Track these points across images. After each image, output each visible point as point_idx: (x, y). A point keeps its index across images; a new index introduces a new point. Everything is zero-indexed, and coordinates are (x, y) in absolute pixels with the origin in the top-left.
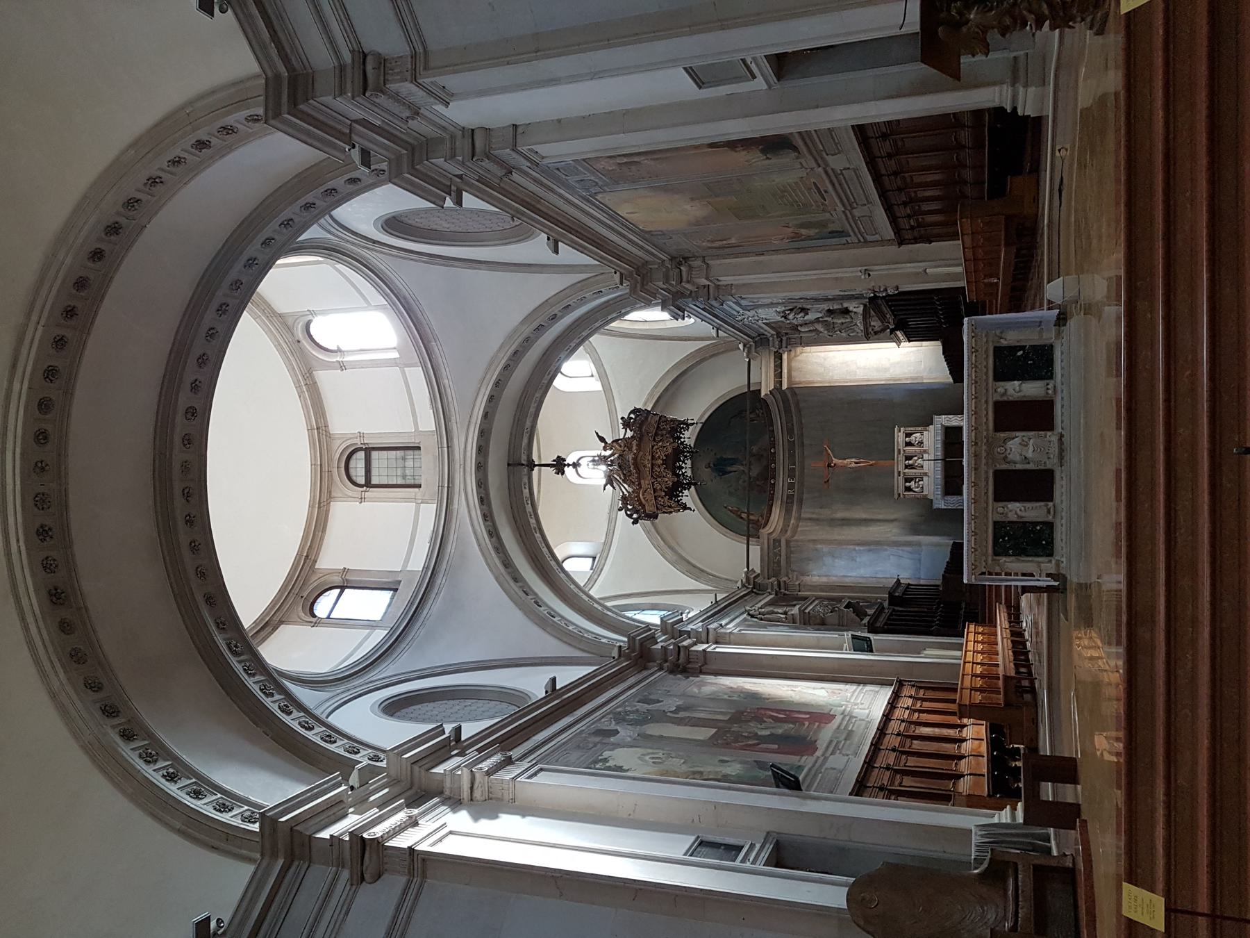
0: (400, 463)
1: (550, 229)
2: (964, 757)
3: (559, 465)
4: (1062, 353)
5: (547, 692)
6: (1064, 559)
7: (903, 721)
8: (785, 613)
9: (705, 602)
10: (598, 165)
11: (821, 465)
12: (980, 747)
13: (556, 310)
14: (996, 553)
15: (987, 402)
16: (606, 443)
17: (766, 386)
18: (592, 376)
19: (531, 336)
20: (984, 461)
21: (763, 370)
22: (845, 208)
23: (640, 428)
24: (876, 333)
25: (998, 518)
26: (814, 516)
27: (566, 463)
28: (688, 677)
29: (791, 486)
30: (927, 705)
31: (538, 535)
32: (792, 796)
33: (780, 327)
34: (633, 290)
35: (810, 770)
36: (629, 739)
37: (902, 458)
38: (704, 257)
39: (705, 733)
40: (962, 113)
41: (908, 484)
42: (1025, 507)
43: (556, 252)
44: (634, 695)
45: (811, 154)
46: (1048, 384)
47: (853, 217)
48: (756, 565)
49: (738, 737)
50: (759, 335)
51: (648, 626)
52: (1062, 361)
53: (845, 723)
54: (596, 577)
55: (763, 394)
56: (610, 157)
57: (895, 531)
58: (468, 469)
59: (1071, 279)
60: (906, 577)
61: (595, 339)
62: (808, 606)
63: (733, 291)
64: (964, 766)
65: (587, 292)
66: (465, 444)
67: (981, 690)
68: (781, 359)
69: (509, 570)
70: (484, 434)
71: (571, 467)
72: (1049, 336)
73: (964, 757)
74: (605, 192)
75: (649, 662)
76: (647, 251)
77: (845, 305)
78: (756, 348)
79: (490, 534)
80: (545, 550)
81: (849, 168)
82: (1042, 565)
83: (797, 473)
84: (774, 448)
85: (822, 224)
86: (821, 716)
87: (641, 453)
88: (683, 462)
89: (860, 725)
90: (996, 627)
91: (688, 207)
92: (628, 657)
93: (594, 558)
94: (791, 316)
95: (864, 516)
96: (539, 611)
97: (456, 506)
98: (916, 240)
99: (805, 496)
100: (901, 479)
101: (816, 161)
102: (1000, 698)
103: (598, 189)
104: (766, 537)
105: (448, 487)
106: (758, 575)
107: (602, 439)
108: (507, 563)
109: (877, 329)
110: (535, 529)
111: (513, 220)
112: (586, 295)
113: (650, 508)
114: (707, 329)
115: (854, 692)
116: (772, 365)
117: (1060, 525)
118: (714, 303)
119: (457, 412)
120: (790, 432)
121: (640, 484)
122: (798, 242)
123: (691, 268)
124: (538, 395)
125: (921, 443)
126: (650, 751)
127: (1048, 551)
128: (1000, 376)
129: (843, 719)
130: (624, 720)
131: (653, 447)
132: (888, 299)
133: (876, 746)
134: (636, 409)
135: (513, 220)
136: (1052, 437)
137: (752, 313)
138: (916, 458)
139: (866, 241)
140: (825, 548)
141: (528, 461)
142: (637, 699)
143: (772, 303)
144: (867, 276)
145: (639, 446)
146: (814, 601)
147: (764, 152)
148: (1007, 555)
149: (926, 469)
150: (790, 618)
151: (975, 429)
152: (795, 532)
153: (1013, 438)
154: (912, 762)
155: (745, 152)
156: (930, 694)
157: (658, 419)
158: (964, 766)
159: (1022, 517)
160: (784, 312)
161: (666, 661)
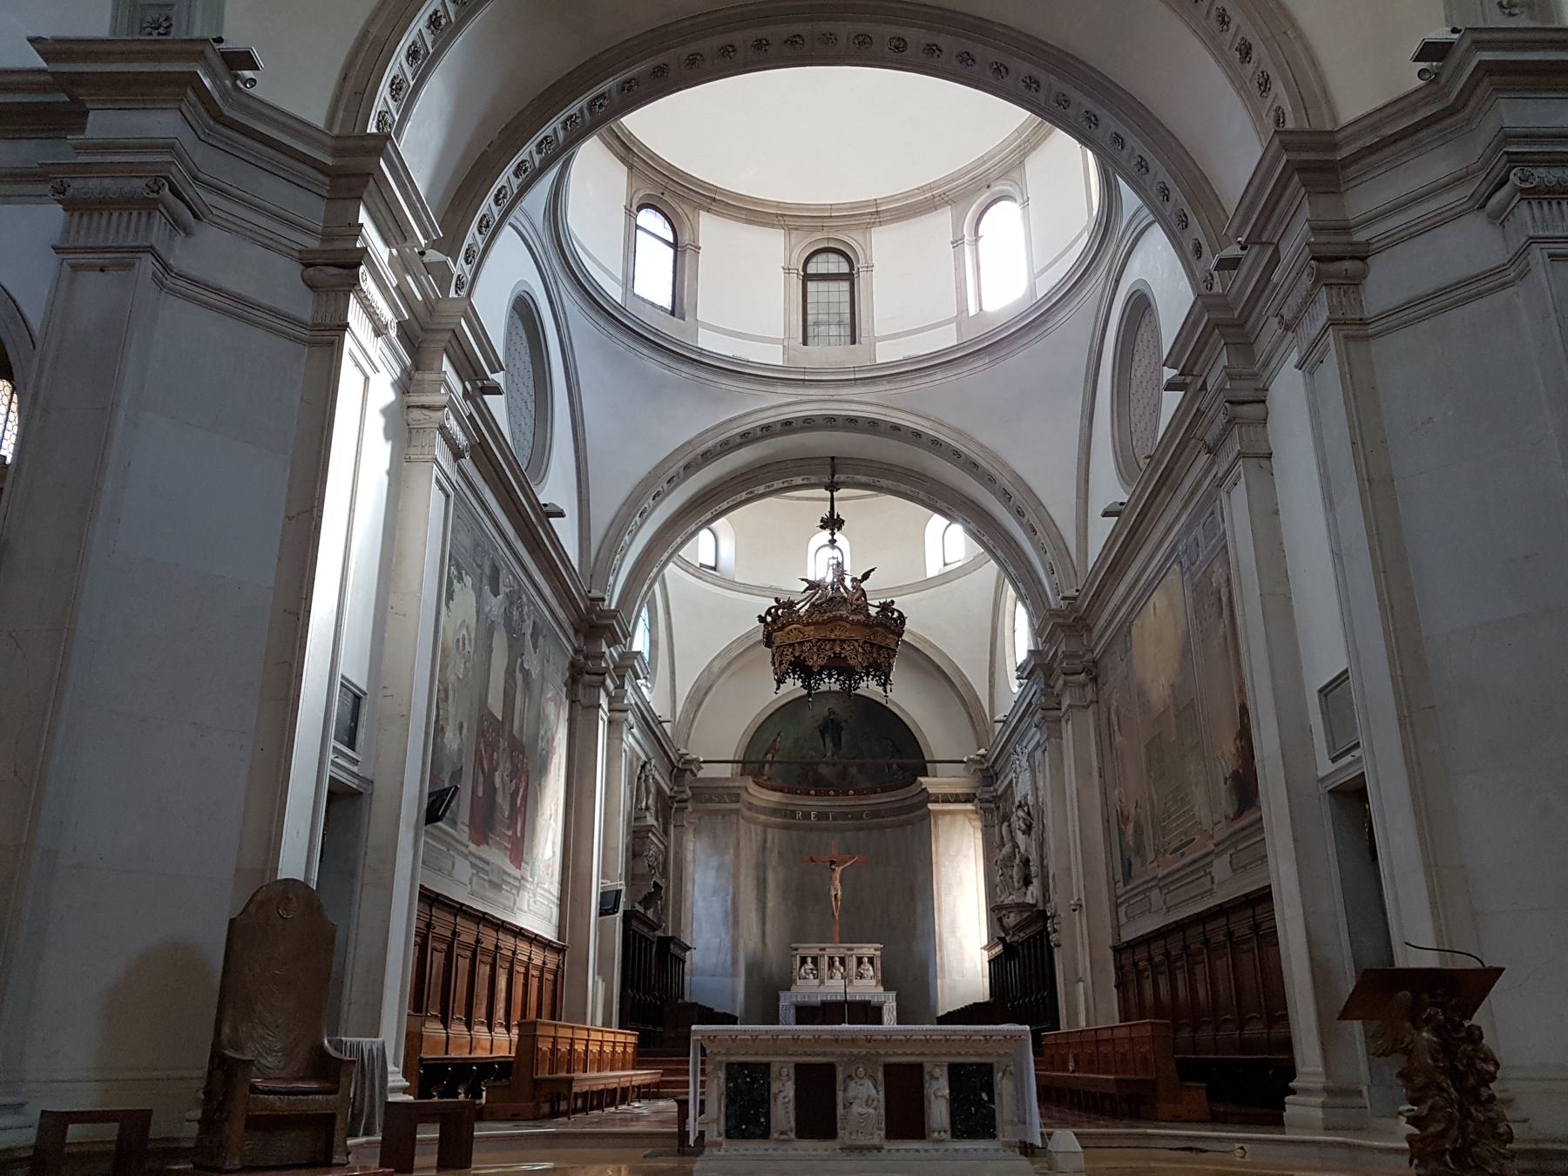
0: (835, 318)
1: (1135, 506)
2: (469, 1028)
3: (833, 523)
4: (985, 1150)
5: (545, 505)
6: (722, 1152)
7: (514, 953)
8: (647, 808)
9: (660, 707)
10: (1218, 564)
11: (834, 852)
12: (483, 1049)
13: (1030, 516)
14: (729, 1066)
15: (922, 1054)
16: (861, 581)
17: (932, 784)
18: (945, 565)
19: (997, 485)
20: (847, 1051)
21: (953, 779)
22: (1160, 880)
23: (880, 624)
24: (1000, 920)
25: (774, 1070)
26: (769, 844)
27: (836, 530)
28: (566, 685)
30: (534, 983)
31: (744, 496)
32: (419, 812)
33: (1006, 801)
34: (1054, 614)
35: (452, 836)
36: (487, 609)
37: (843, 952)
38: (1097, 702)
39: (496, 705)
40: (1288, 1026)
41: (809, 960)
42: (788, 1102)
43: (1106, 514)
44: (542, 616)
45: (1232, 835)
46: (945, 1132)
47: (1150, 889)
48: (707, 772)
49: (492, 747)
50: (996, 774)
51: (629, 635)
52: (976, 1150)
53: (511, 881)
54: (691, 570)
55: (922, 779)
56: (1228, 580)
57: (751, 945)
58: (828, 406)
59: (1080, 1162)
60: (694, 959)
61: (992, 567)
62: (657, 837)
63: (1053, 740)
64: (458, 1029)
65: (1052, 555)
66: (861, 402)
67: (554, 1050)
68: (967, 801)
69: (700, 460)
70: (873, 426)
71: (830, 537)
72: (1006, 1133)
73: (469, 1028)
74: (1183, 574)
75: (585, 637)
76: (1105, 629)
77: (1035, 881)
78: (980, 770)
79: (745, 435)
80: (725, 505)
81: (1213, 883)
82: (715, 1126)
83: (823, 822)
84: (855, 794)
85: (1139, 849)
86: (519, 850)
87: (848, 626)
88: (837, 680)
89: (508, 899)
90: (633, 1069)
91: (1163, 680)
92: (590, 610)
93: (714, 569)
94: (1021, 813)
95: (770, 905)
96: (648, 498)
97: (780, 390)
98: (1119, 968)
100: (816, 952)
101: (1222, 842)
102: (543, 1074)
103: (1186, 565)
104: (742, 784)
105: (804, 380)
106: (695, 775)
107: (866, 576)
108: (708, 457)
109: (1005, 920)
110: (752, 492)
111: (1147, 457)
112: (1048, 554)
113: (778, 637)
114: (1004, 709)
115: (550, 893)
116: (959, 791)
117: (766, 1147)
118: (1038, 717)
119: (899, 391)
120: (875, 814)
121: (808, 624)
122: (1116, 821)
123: (1083, 686)
124: (922, 495)
125: (861, 976)
126: (473, 636)
127: (733, 1132)
128: (955, 1071)
129: (516, 878)
130: (511, 604)
131: (857, 641)
132: (1044, 934)
133: (482, 919)
134: (905, 619)
135: (1147, 457)
136: (878, 1137)
137: (1025, 764)
138: (842, 970)
139: (1118, 906)
140: (729, 858)
141: (837, 483)
142: (537, 620)
143: (1037, 789)
144: (1073, 907)
145: (858, 623)
146: (663, 844)
147: (1235, 775)
148: (728, 1080)
149: (828, 982)
150: (641, 814)
151: (888, 1039)
152: (747, 820)
153: (875, 1088)
154: (463, 964)
155: (1234, 751)
156: (547, 987)
157: (892, 647)
158: (458, 1029)
159: (776, 1098)
160: (1027, 804)
161: (586, 658)
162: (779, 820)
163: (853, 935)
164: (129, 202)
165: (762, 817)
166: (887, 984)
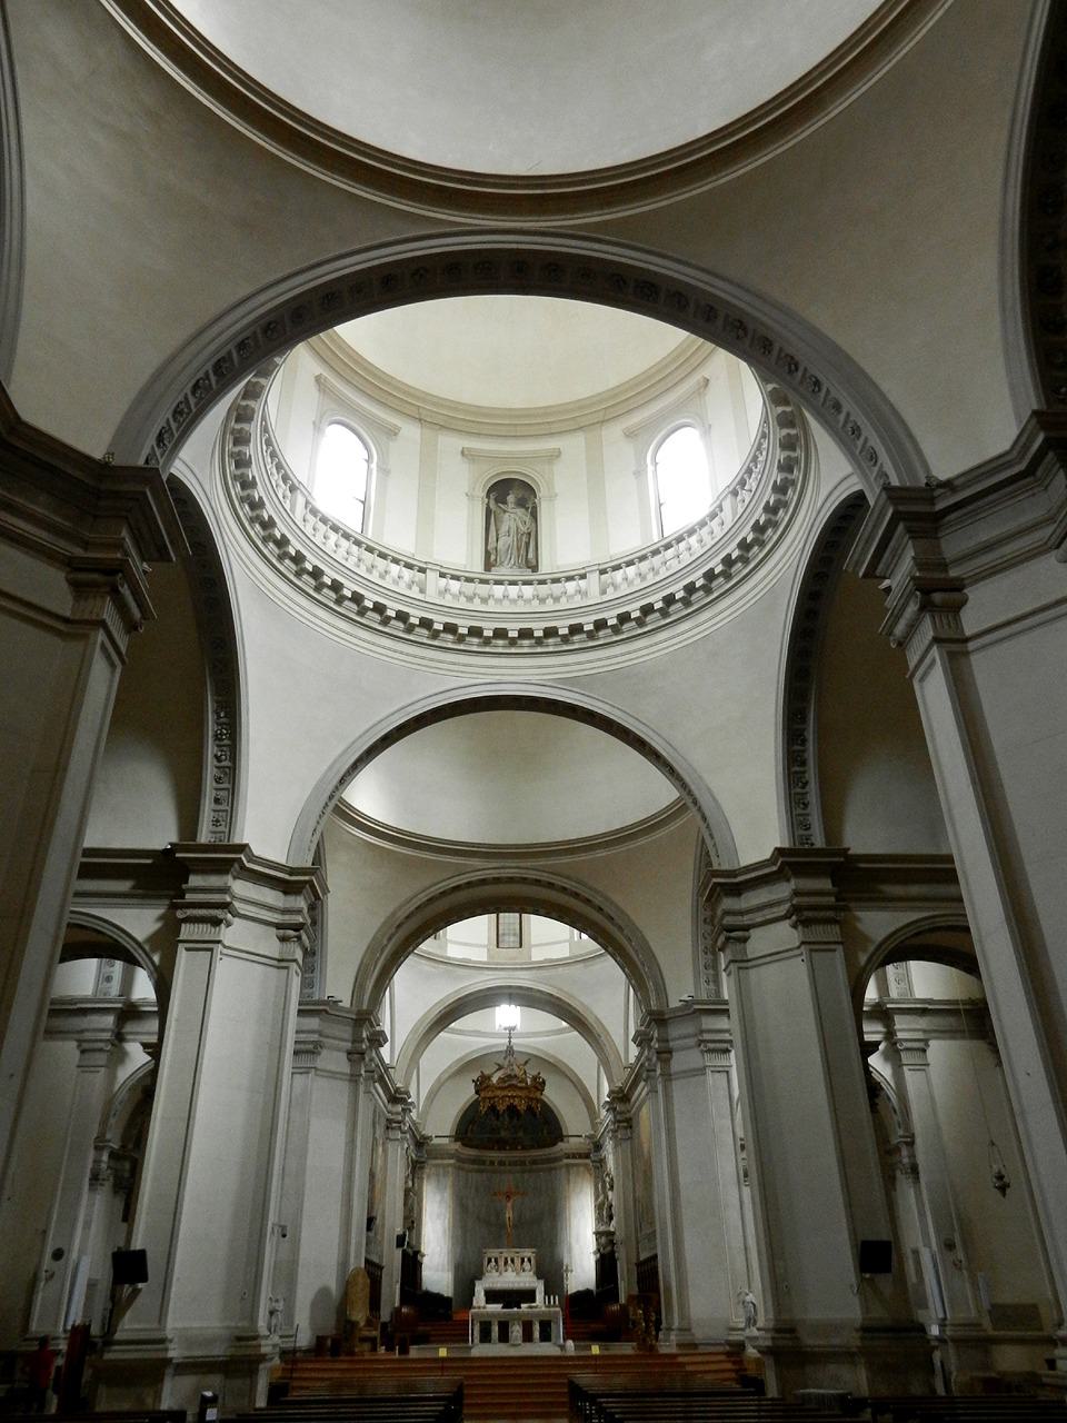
29: (492, 1163)
48: (436, 1141)
60: (426, 1261)
99: (484, 1175)
100: (497, 1255)
120: (534, 1162)
123: (626, 1128)
132: (613, 1252)
149: (504, 1274)
162: (476, 1167)
163: (520, 1244)
164: (307, 1052)
165: (466, 1166)
166: (539, 1275)
